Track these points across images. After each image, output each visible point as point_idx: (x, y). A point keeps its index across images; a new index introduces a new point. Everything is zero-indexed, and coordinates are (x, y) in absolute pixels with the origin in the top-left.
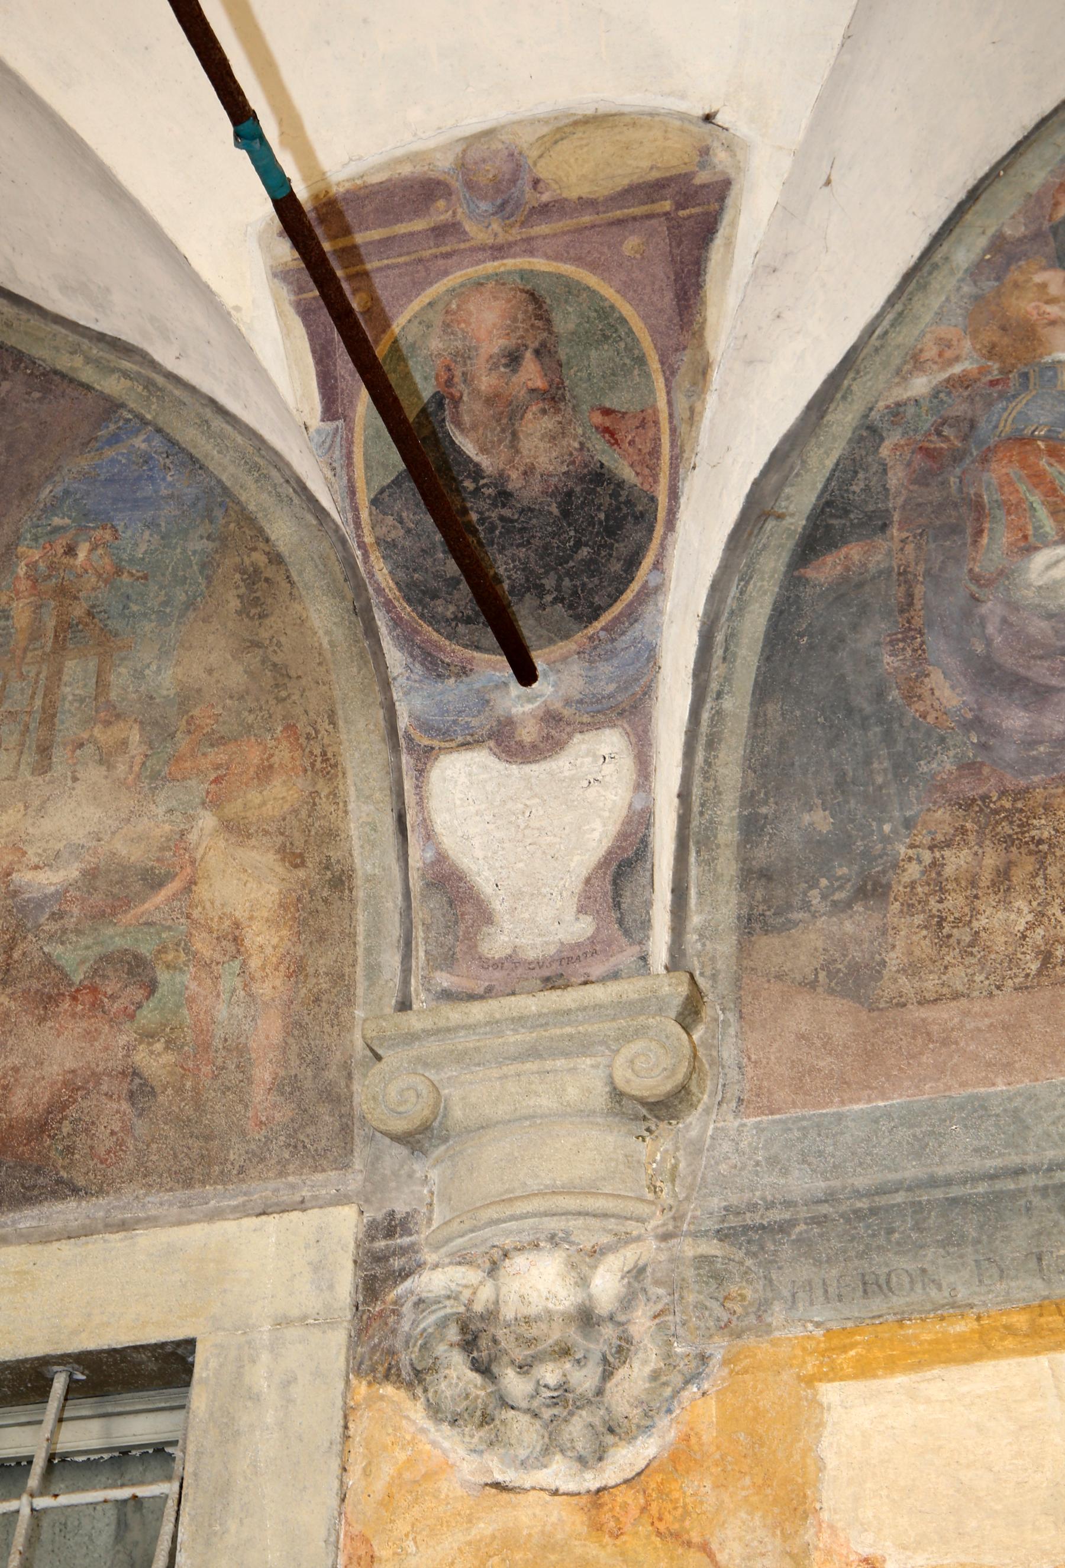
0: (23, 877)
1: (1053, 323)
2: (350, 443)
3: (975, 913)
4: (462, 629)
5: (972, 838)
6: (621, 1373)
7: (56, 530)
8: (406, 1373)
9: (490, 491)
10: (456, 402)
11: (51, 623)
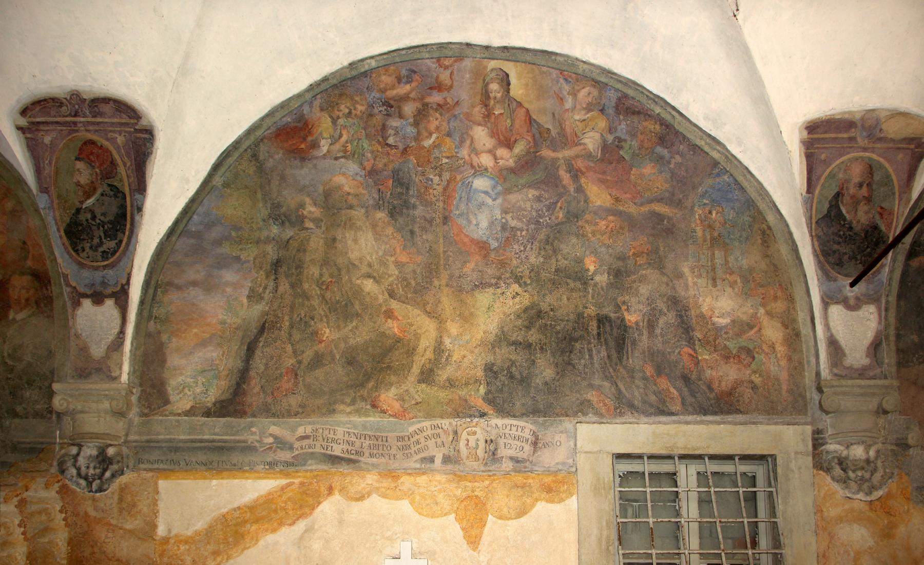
0: (715, 319)
2: (812, 202)
4: (836, 267)
6: (875, 475)
7: (705, 204)
8: (825, 469)
9: (847, 226)
10: (843, 195)
11: (709, 237)
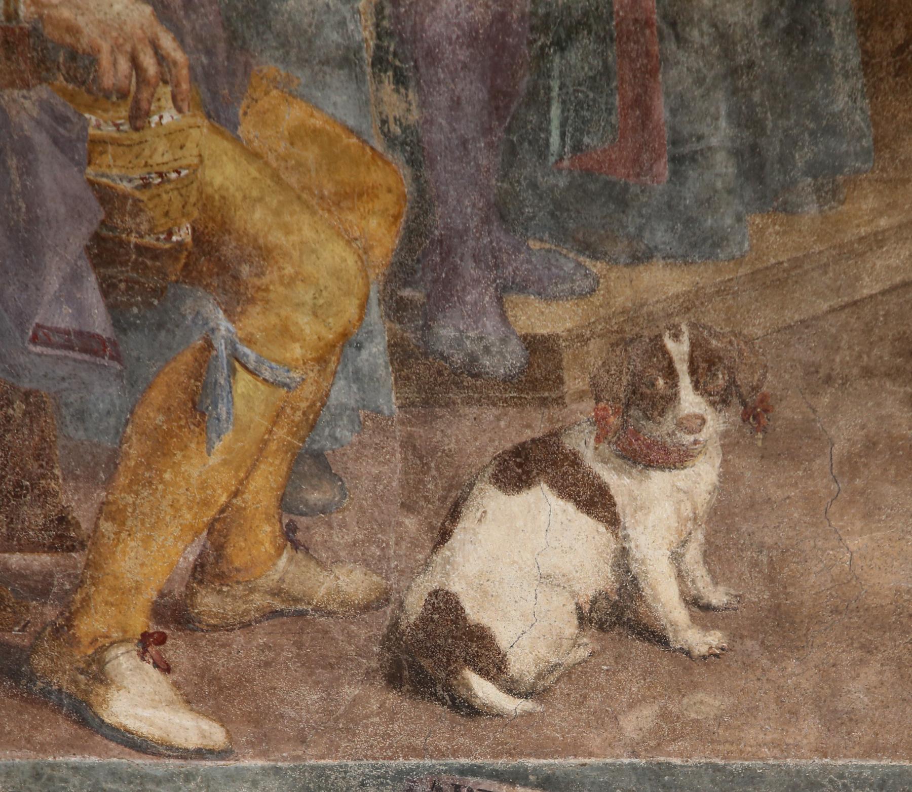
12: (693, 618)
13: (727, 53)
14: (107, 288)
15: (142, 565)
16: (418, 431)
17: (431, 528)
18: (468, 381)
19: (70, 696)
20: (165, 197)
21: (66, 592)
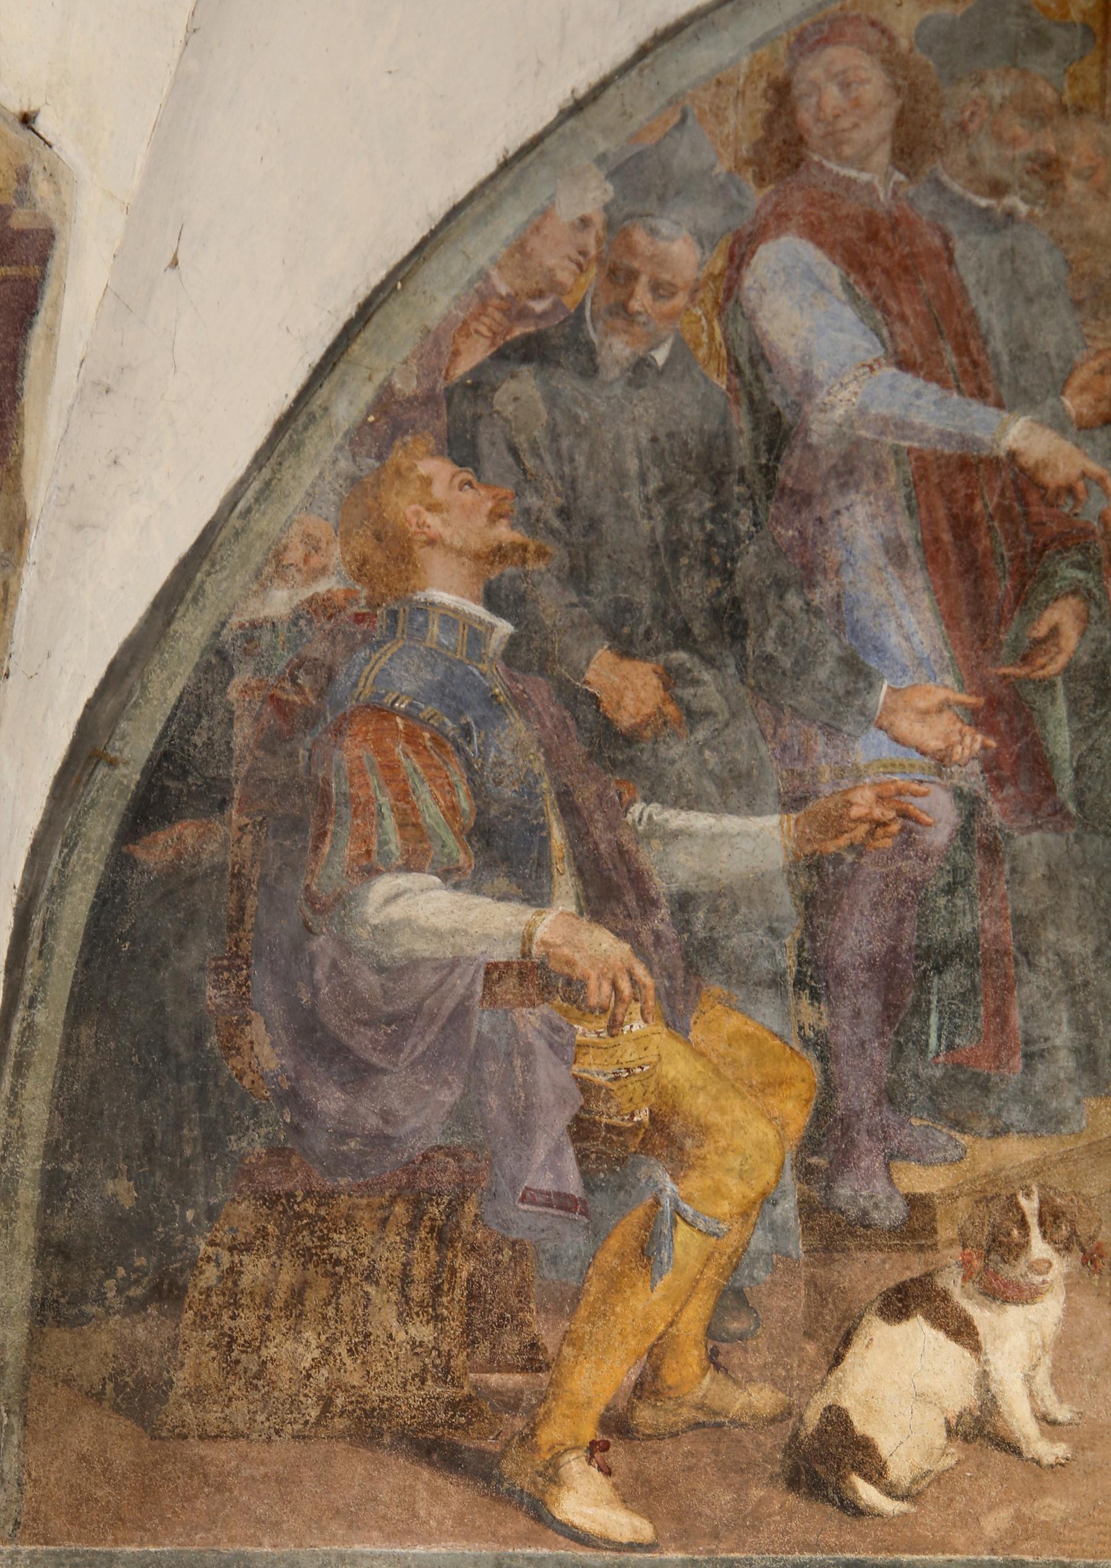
1: (431, 542)
3: (265, 1338)
5: (272, 1244)
12: (1042, 1432)
13: (1068, 975)
14: (582, 1158)
15: (594, 1383)
16: (820, 1272)
17: (828, 1352)
18: (861, 1231)
19: (529, 1495)
20: (630, 1087)
21: (532, 1406)
